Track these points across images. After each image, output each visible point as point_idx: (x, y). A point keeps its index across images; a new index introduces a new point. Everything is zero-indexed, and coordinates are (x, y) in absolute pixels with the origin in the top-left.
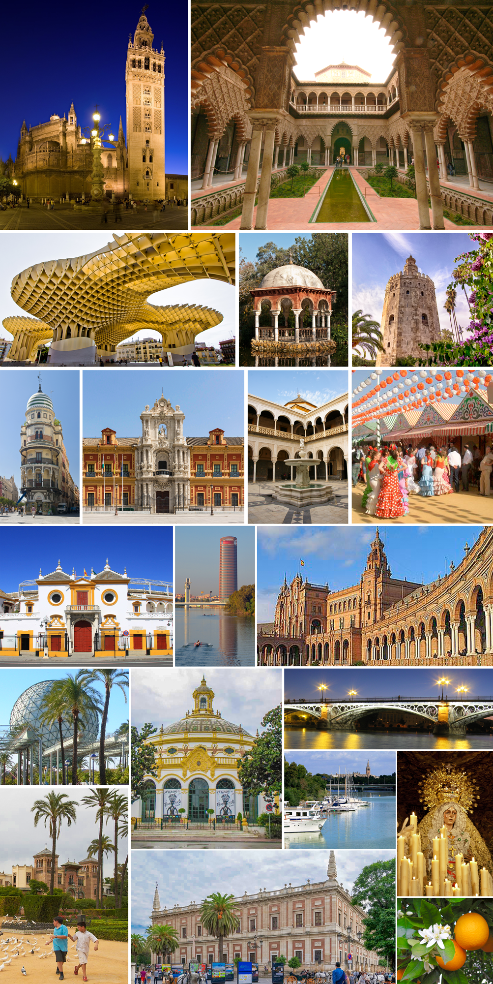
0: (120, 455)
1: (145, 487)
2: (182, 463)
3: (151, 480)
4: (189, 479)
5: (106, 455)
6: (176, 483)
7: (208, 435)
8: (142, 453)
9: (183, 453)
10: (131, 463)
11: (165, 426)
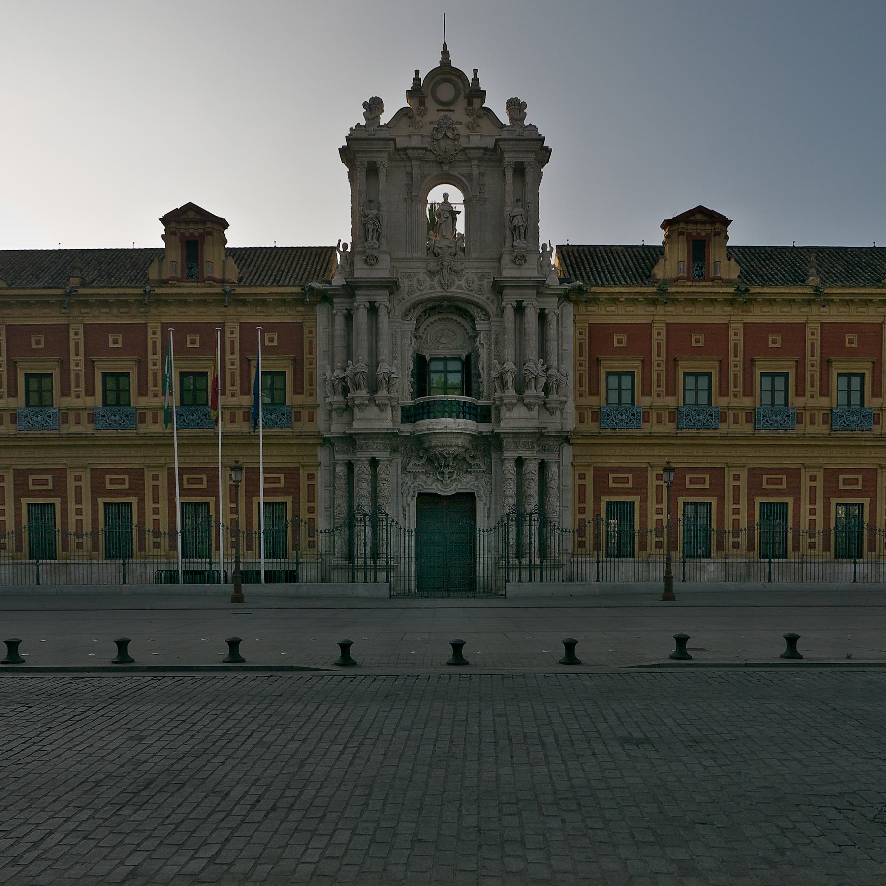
0: (247, 331)
1: (363, 471)
2: (534, 365)
3: (391, 438)
4: (566, 439)
5: (182, 329)
6: (510, 455)
7: (657, 238)
8: (349, 317)
10: (298, 364)
11: (456, 197)
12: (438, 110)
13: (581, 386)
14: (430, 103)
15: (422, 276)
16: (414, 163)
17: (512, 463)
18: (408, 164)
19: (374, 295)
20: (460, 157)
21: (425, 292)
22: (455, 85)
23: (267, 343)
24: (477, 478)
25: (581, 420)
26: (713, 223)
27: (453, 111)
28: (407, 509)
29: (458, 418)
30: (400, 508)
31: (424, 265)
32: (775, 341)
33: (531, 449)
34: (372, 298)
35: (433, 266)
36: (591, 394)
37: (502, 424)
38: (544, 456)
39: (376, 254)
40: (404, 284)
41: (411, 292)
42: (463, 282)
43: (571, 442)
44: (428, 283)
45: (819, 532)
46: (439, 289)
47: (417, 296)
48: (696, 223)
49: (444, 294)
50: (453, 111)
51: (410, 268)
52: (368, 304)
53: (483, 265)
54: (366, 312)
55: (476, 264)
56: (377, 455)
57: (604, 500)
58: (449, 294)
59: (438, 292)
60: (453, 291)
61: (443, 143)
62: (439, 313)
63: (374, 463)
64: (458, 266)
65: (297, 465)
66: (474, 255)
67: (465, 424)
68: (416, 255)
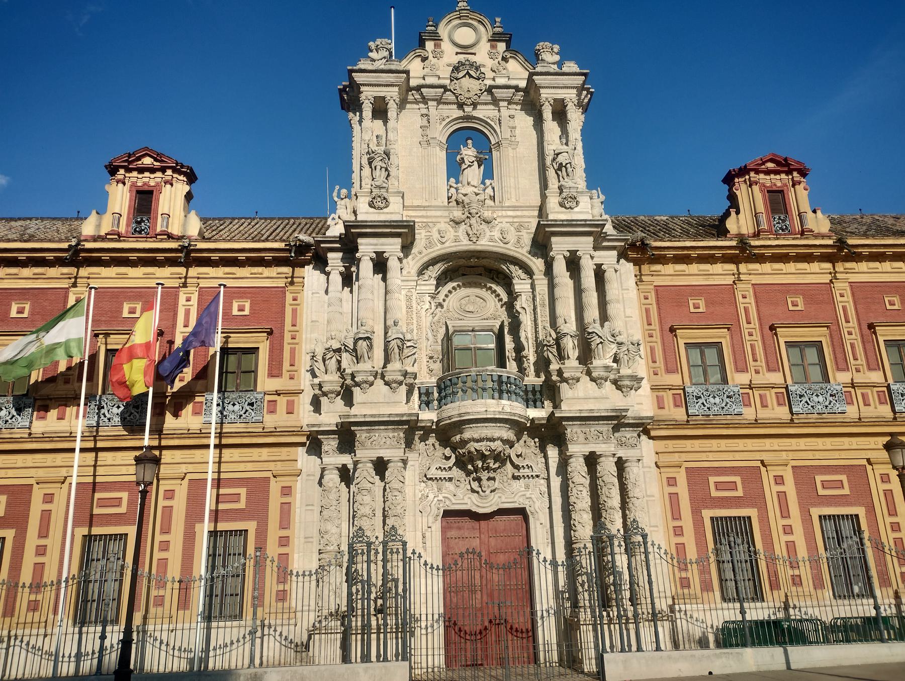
6: (578, 449)
9: (599, 274)
12: (457, 53)
13: (654, 362)
14: (446, 45)
15: (443, 225)
16: (430, 103)
17: (582, 460)
18: (422, 105)
19: (382, 245)
20: (486, 97)
21: (447, 244)
22: (475, 29)
23: (235, 312)
24: (527, 487)
25: (661, 407)
26: (789, 172)
27: (474, 54)
28: (428, 535)
29: (500, 398)
30: (419, 535)
31: (446, 213)
33: (607, 441)
34: (380, 249)
35: (458, 214)
36: (668, 371)
37: (564, 406)
38: (621, 453)
39: (385, 195)
40: (421, 235)
41: (430, 244)
42: (497, 234)
43: (653, 433)
44: (451, 233)
47: (438, 250)
48: (768, 172)
49: (473, 247)
50: (474, 54)
51: (427, 217)
52: (374, 255)
53: (519, 213)
54: (371, 264)
56: (386, 454)
57: (707, 514)
58: (479, 248)
59: (465, 245)
60: (483, 244)
61: (466, 82)
62: (464, 275)
63: (381, 466)
64: (487, 214)
65: (269, 474)
68: (434, 203)
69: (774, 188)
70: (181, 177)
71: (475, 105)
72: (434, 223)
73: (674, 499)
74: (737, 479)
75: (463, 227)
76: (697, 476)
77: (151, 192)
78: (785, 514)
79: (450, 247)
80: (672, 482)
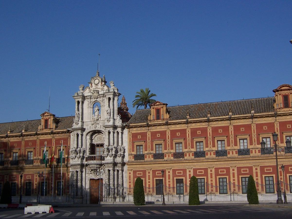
31: (90, 123)
32: (199, 132)
42: (99, 126)
45: (241, 186)
46: (94, 128)
49: (95, 129)
55: (102, 122)
56: (78, 170)
58: (96, 129)
59: (94, 129)
66: (102, 120)
67: (96, 162)
69: (158, 109)
70: (52, 116)
71: (97, 98)
72: (89, 125)
73: (130, 177)
74: (142, 173)
75: (94, 125)
76: (135, 172)
77: (47, 120)
78: (149, 179)
79: (92, 130)
80: (130, 173)
